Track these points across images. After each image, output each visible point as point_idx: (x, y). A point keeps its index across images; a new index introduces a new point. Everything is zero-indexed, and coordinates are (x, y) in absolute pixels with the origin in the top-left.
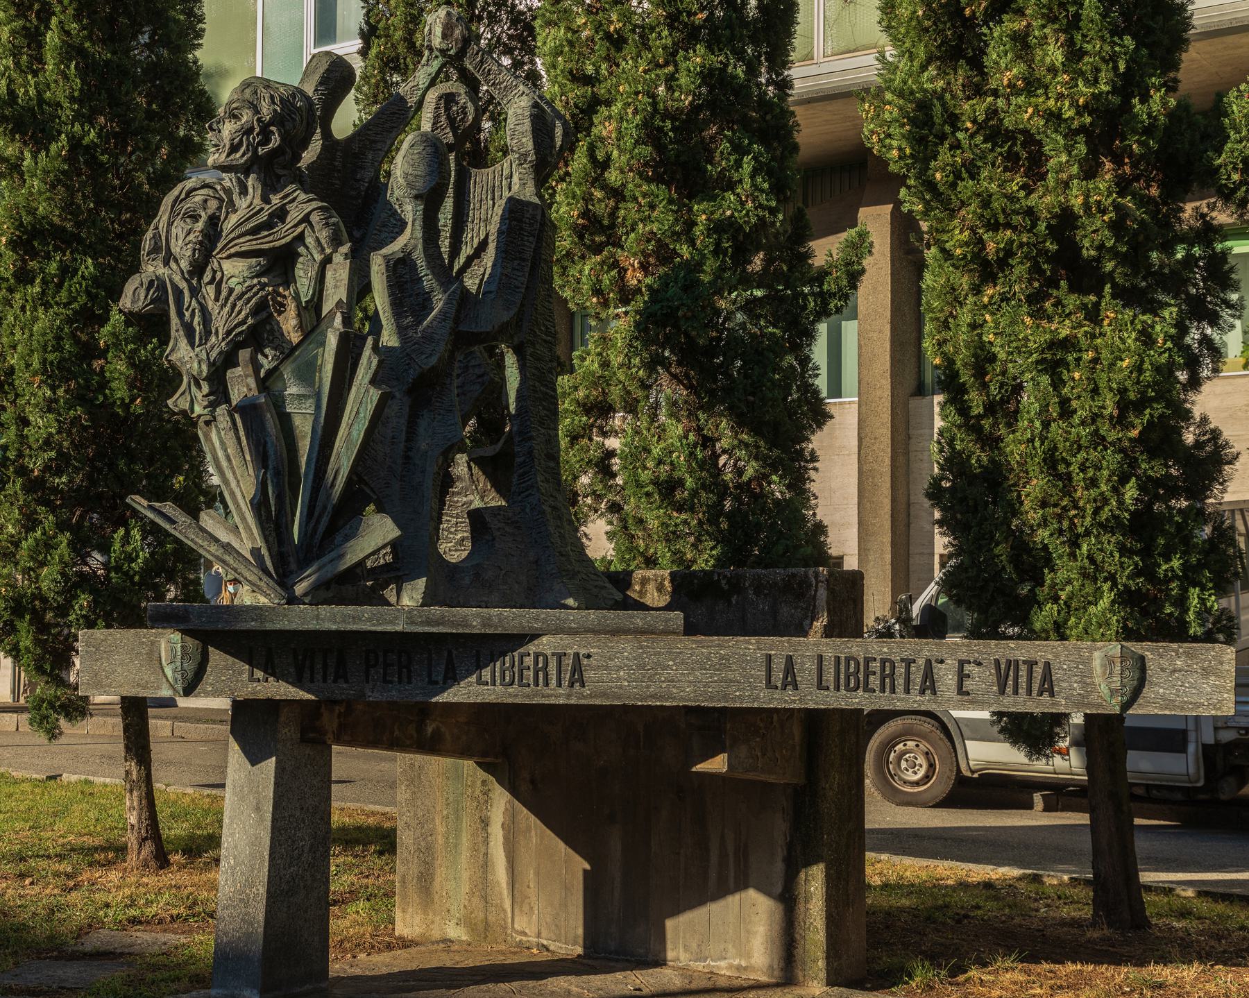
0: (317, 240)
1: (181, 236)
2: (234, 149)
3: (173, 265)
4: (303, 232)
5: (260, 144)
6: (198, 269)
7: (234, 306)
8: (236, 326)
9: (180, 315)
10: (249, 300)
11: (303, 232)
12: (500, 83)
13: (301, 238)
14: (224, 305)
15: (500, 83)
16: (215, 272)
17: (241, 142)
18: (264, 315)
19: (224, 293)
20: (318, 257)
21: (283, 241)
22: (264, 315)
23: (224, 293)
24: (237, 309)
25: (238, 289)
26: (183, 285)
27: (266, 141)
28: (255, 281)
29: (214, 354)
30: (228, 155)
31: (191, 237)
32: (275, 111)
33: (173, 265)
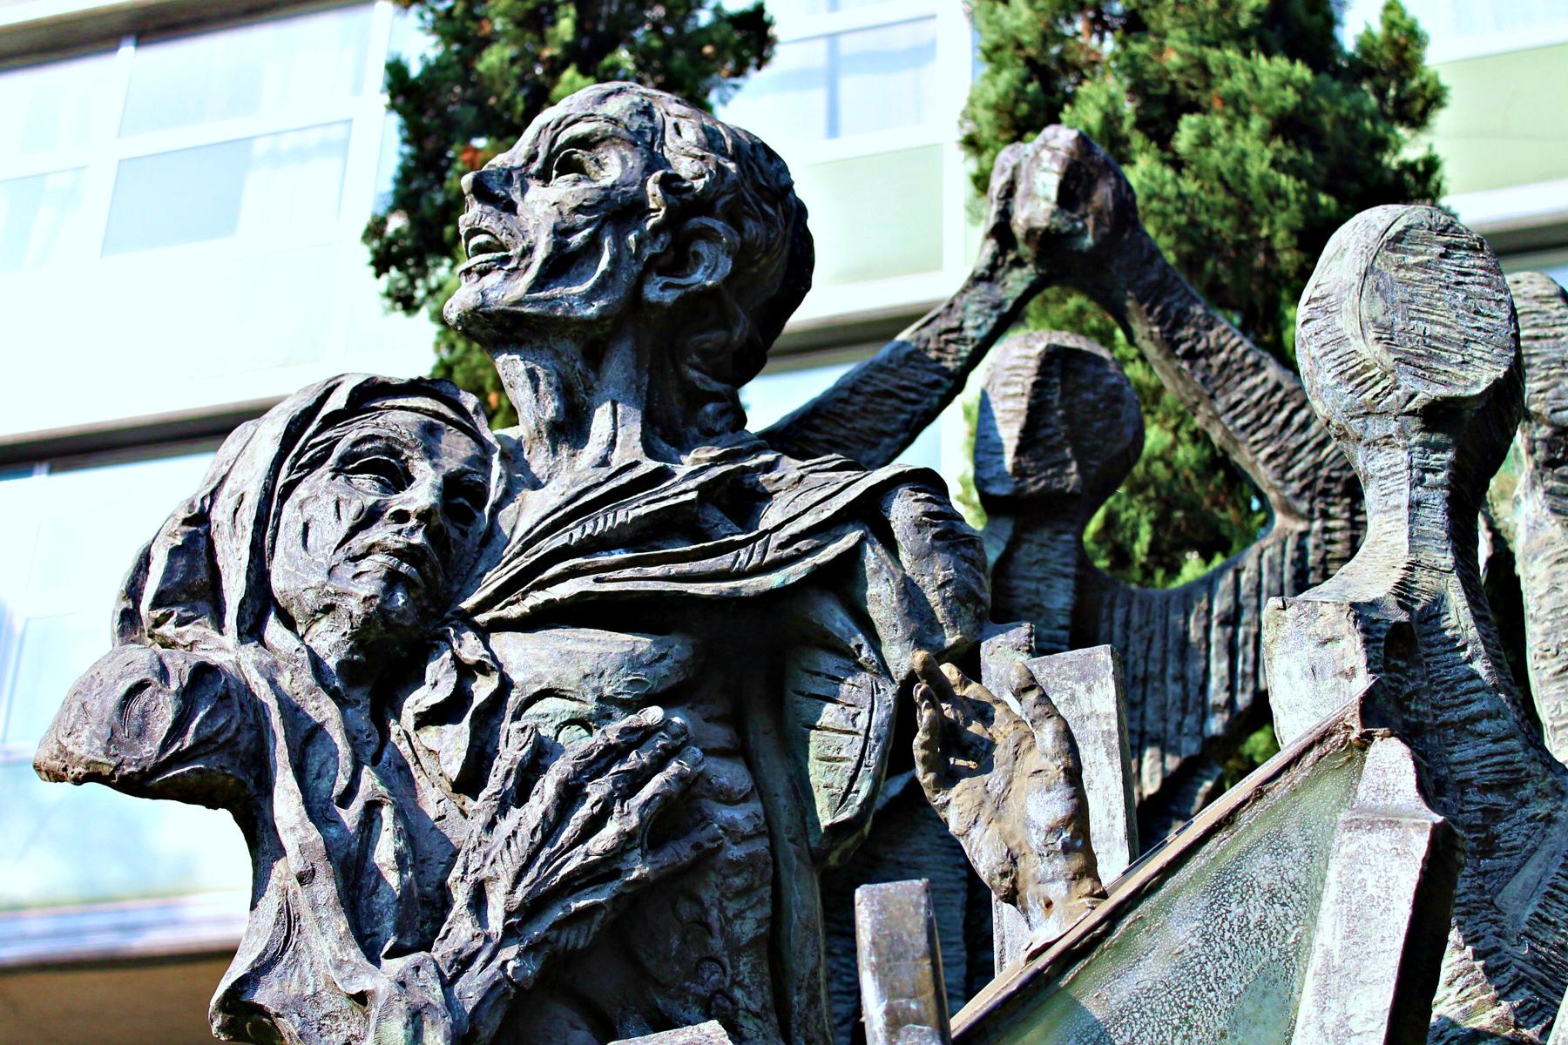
0: (910, 592)
1: (329, 531)
2: (561, 265)
3: (274, 630)
4: (855, 553)
5: (654, 266)
6: (379, 667)
7: (570, 794)
8: (573, 884)
9: (318, 811)
10: (634, 781)
11: (853, 556)
12: (1209, 353)
13: (842, 579)
14: (520, 794)
15: (1209, 353)
16: (466, 672)
17: (592, 248)
18: (682, 851)
19: (511, 750)
20: (903, 658)
21: (775, 580)
22: (682, 851)
23: (511, 750)
24: (583, 812)
25: (577, 743)
26: (324, 710)
27: (677, 261)
28: (654, 714)
29: (471, 987)
30: (539, 283)
31: (382, 533)
32: (721, 170)
33: (274, 630)
